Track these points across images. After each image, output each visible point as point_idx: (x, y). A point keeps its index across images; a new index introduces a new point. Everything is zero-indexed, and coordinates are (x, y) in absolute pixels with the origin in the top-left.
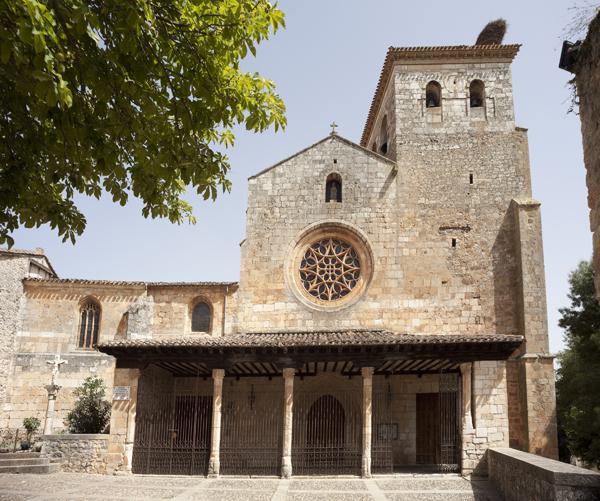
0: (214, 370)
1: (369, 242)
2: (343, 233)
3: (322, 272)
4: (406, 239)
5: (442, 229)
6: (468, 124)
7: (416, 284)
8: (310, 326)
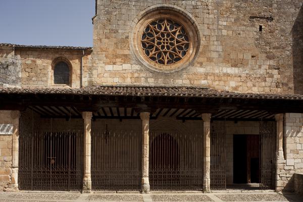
0: (84, 113)
1: (196, 23)
3: (159, 43)
4: (225, 23)
7: (233, 56)
8: (151, 82)
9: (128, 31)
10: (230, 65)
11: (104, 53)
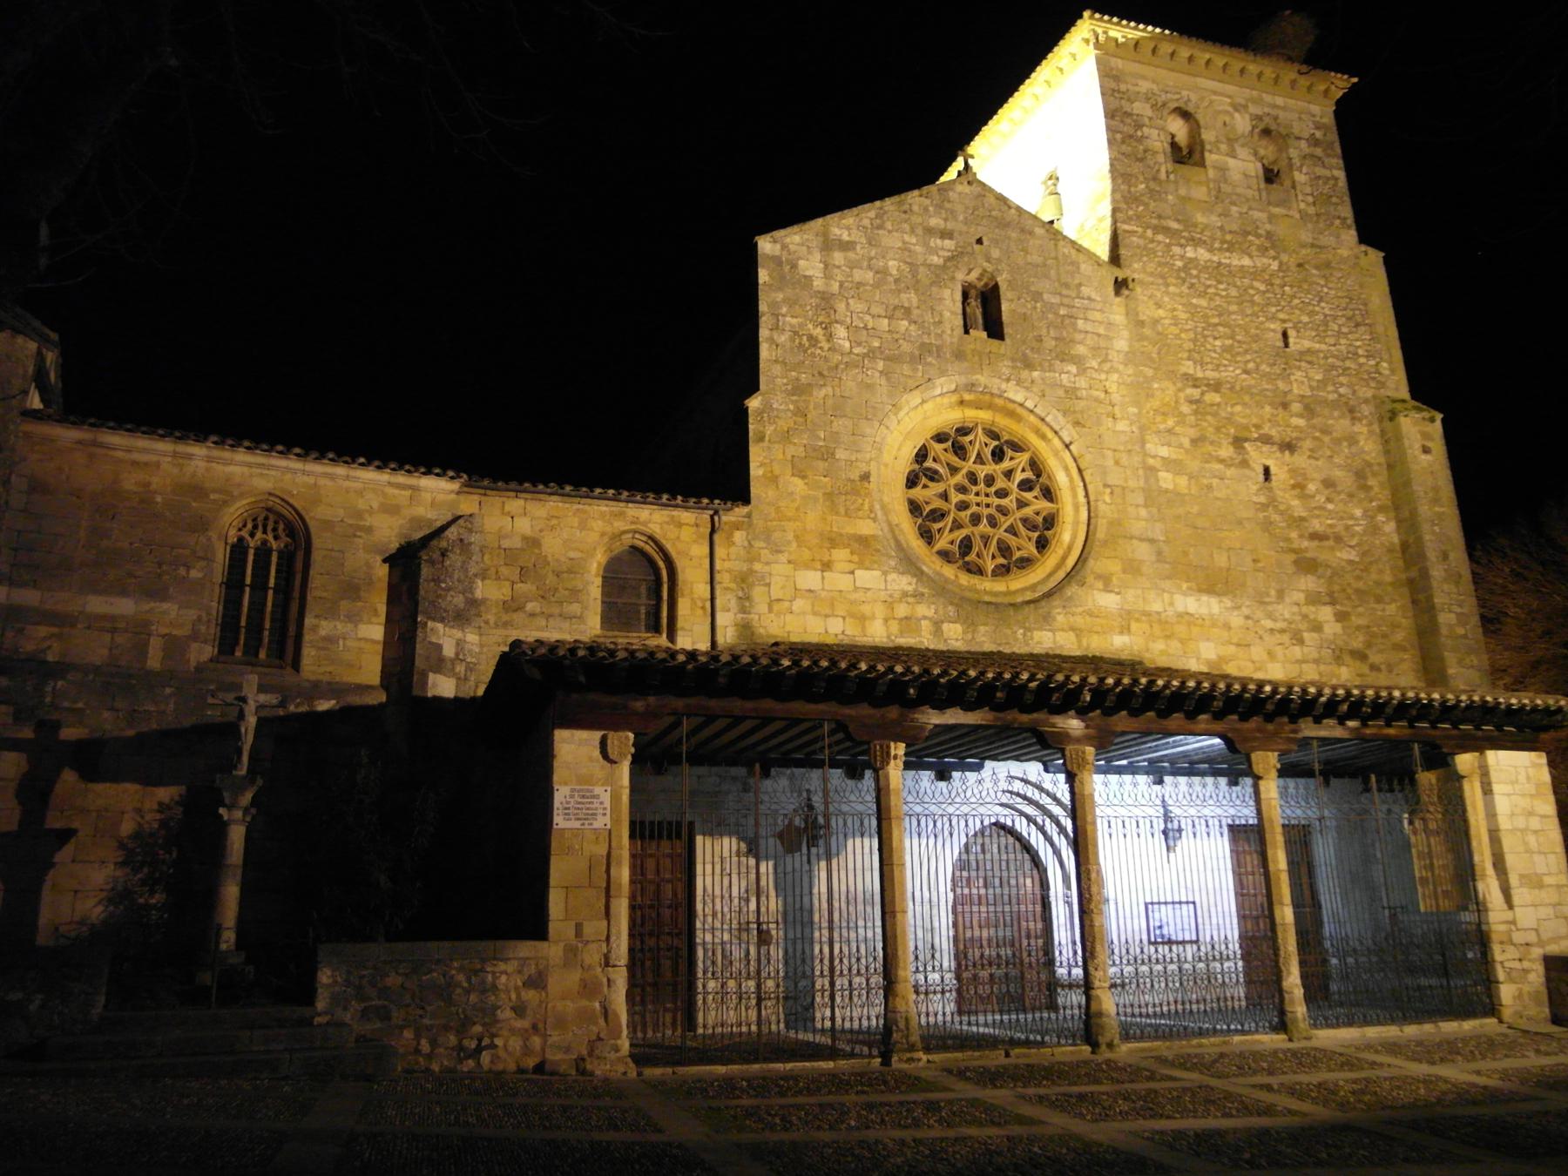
2: (1011, 414)
4: (1164, 452)
8: (955, 637)
10: (1193, 585)
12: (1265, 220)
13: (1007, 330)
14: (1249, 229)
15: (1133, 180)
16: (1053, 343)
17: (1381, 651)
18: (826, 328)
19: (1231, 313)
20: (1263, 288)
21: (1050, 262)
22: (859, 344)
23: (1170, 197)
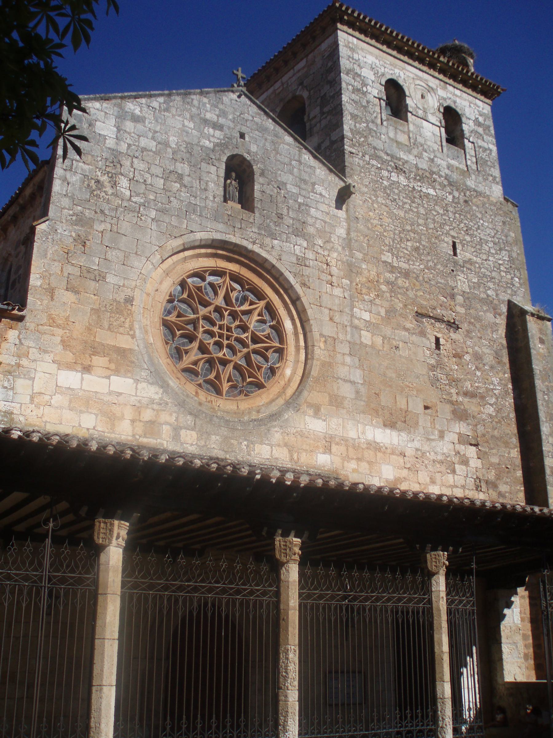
1: (304, 300)
4: (366, 316)
5: (419, 315)
6: (444, 164)
7: (385, 400)
9: (134, 283)
10: (380, 420)
11: (60, 332)
12: (445, 167)
13: (257, 204)
14: (435, 170)
15: (359, 119)
16: (291, 221)
17: (506, 483)
18: (112, 177)
19: (419, 225)
20: (441, 212)
21: (294, 163)
22: (138, 195)
23: (382, 136)
